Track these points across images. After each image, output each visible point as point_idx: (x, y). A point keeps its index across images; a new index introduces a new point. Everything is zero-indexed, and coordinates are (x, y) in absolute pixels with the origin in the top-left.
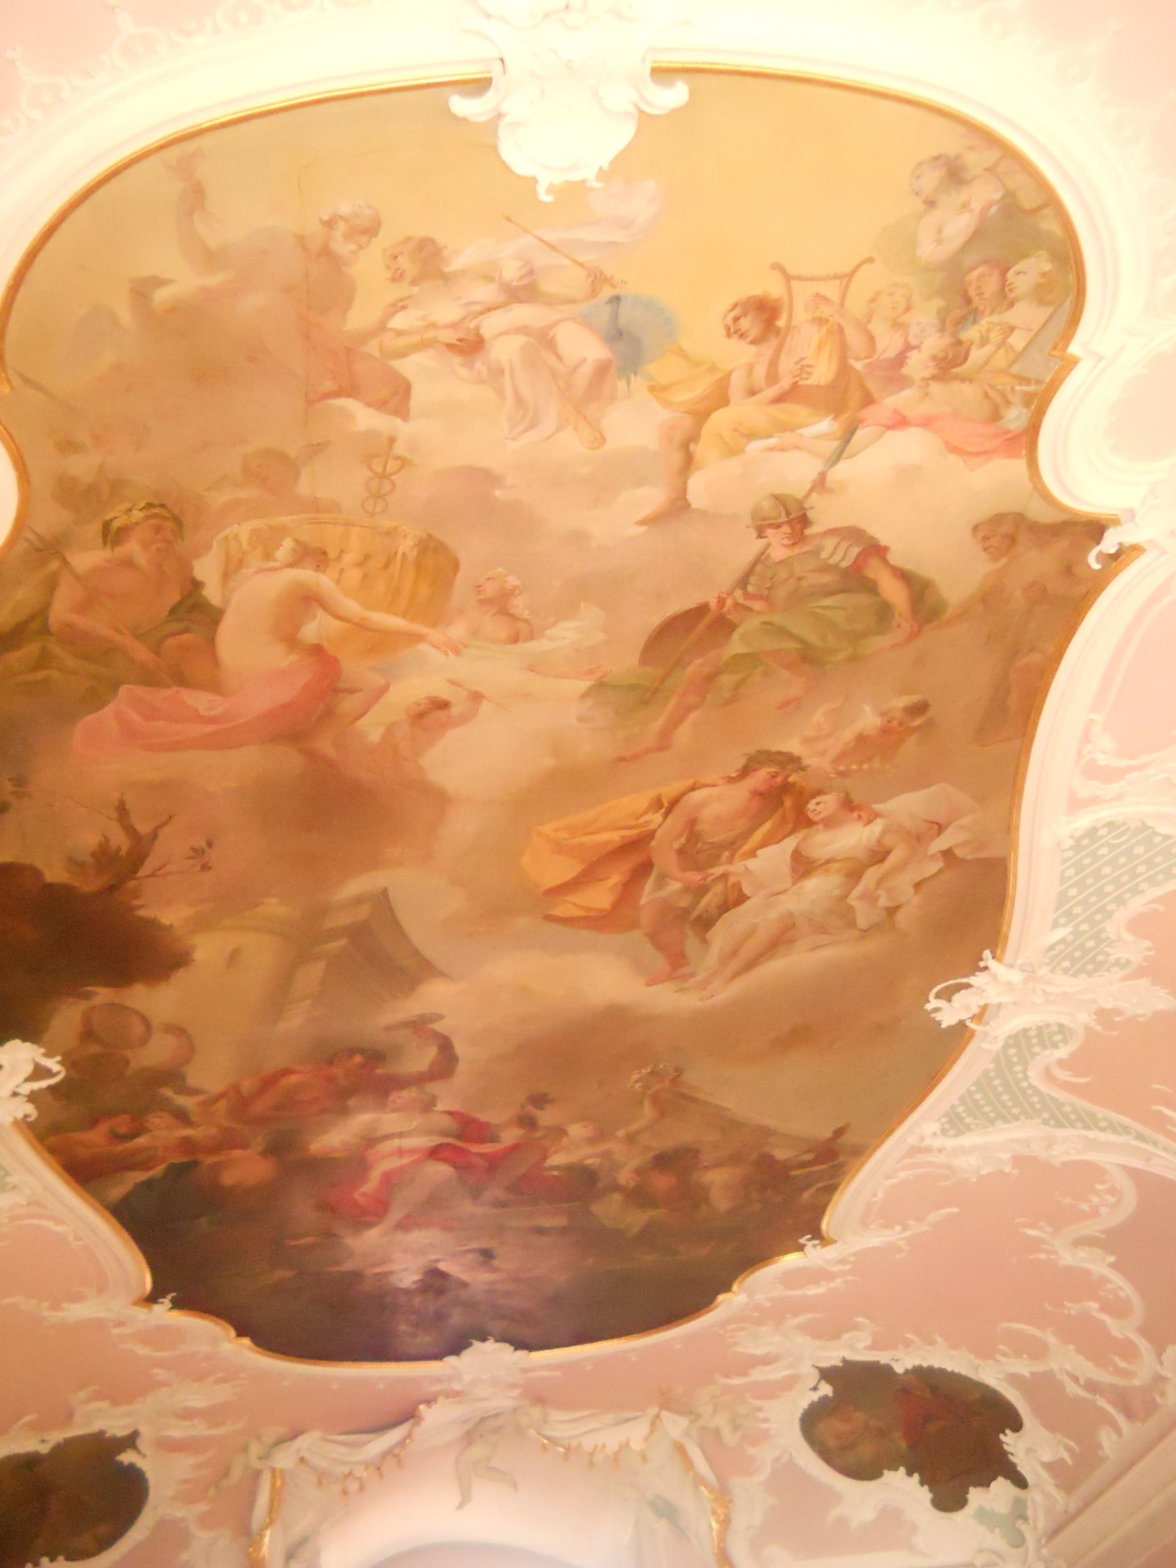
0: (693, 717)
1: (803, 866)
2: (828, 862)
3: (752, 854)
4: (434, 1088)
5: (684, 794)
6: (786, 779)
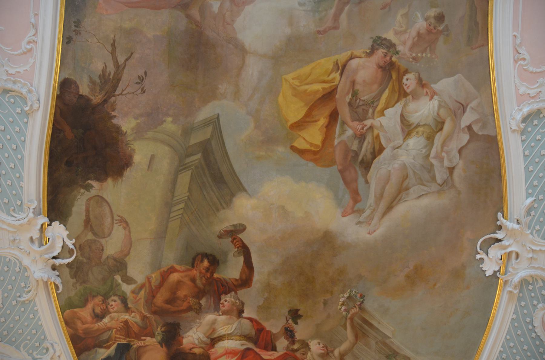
0: (347, 8)
1: (408, 128)
2: (418, 126)
3: (382, 114)
4: (242, 293)
6: (391, 59)
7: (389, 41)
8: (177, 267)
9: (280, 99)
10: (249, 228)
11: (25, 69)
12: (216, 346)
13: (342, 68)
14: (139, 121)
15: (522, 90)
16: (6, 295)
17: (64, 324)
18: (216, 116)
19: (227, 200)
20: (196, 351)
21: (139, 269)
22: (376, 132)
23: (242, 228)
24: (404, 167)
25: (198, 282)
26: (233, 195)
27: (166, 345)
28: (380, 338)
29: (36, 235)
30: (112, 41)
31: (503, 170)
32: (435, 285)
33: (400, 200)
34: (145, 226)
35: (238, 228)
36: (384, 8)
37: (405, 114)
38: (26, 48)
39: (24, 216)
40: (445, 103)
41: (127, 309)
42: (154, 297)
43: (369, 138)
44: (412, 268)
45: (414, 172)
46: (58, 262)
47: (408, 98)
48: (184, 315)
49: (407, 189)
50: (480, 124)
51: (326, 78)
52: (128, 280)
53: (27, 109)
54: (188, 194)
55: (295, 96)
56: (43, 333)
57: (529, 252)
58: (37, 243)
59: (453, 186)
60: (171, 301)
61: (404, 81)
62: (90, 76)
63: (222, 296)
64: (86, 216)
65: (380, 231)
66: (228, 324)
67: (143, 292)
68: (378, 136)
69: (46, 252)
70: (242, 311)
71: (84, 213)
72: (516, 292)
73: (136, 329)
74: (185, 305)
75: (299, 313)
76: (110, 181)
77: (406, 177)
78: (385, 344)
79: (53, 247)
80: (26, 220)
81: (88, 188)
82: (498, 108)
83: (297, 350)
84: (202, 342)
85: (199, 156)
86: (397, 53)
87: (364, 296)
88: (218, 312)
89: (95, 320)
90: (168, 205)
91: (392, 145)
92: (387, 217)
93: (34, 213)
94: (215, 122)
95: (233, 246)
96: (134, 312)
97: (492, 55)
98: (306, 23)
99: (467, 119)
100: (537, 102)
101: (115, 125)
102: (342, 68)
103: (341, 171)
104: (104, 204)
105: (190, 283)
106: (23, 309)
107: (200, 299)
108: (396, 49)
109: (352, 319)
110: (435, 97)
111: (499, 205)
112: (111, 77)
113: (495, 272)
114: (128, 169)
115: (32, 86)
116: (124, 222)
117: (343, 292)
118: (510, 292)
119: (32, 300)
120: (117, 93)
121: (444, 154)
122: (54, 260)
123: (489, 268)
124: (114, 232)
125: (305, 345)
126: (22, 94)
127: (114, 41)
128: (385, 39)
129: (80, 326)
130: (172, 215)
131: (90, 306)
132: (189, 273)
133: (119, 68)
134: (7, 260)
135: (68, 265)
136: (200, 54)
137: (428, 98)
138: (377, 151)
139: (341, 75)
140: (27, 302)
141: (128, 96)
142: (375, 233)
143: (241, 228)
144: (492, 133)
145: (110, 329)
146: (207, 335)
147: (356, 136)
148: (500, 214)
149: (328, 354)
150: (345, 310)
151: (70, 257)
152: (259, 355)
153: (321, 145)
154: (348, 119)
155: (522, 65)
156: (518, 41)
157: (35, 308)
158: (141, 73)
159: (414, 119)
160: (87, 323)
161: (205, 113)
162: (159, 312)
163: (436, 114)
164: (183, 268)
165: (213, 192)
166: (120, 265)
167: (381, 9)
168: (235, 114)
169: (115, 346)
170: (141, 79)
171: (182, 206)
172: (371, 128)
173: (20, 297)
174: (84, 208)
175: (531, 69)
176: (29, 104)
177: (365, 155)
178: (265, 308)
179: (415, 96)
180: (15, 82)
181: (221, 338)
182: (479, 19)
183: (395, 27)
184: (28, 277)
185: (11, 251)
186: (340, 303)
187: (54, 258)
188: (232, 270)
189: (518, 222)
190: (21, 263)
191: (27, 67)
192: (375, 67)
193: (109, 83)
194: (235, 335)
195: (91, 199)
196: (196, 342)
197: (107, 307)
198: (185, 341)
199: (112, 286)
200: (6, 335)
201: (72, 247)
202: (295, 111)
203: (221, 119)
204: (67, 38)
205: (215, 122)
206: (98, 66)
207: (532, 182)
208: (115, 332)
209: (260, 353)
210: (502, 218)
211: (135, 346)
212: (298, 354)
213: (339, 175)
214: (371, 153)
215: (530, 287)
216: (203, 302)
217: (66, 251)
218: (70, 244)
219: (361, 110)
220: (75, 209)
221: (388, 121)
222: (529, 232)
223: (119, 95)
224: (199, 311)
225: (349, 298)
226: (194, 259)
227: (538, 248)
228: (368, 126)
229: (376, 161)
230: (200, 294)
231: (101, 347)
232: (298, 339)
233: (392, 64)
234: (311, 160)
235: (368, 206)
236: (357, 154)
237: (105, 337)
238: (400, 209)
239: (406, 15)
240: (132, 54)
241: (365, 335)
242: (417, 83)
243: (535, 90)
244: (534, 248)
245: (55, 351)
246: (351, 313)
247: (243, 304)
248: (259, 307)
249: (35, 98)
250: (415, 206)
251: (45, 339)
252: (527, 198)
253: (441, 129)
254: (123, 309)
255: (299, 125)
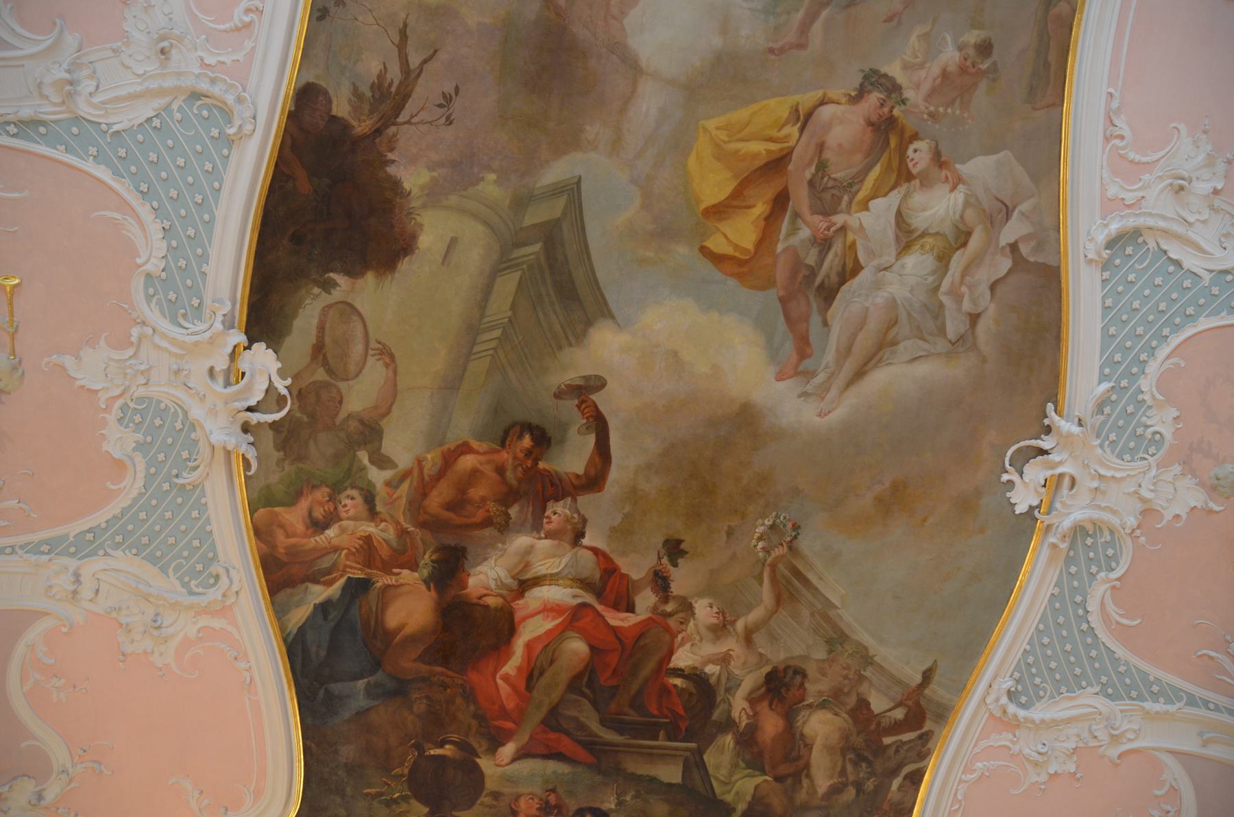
0: (825, 13)
1: (907, 236)
2: (924, 234)
4: (584, 501)
5: (816, 107)
7: (892, 80)
8: (475, 444)
9: (692, 161)
10: (611, 385)
11: (235, 58)
12: (527, 594)
13: (804, 118)
14: (435, 174)
15: (1112, 191)
16: (153, 470)
17: (252, 533)
18: (576, 180)
19: (578, 330)
20: (491, 601)
21: (404, 443)
22: (851, 237)
23: (597, 384)
24: (892, 303)
25: (509, 474)
26: (589, 323)
27: (436, 587)
28: (820, 607)
29: (221, 364)
30: (401, 25)
31: (1064, 329)
32: (925, 520)
33: (880, 361)
34: (425, 364)
35: (592, 383)
36: (889, 19)
37: (904, 211)
38: (241, 20)
39: (203, 327)
40: (977, 199)
41: (373, 514)
42: (425, 495)
43: (837, 247)
44: (887, 485)
45: (909, 315)
46: (255, 418)
47: (913, 183)
48: (476, 533)
49: (894, 343)
50: (1033, 243)
51: (774, 133)
52: (382, 461)
53: (231, 131)
54: (510, 313)
55: (718, 158)
56: (213, 547)
57: (1093, 479)
58: (221, 380)
59: (975, 347)
60: (454, 506)
61: (910, 152)
62: (354, 84)
63: (550, 504)
64: (318, 337)
65: (839, 414)
66: (554, 556)
67: (405, 486)
68: (854, 243)
69: (236, 397)
70: (581, 535)
71: (314, 332)
72: (1064, 546)
73: (384, 552)
74: (480, 515)
75: (683, 546)
76: (370, 277)
77: (894, 322)
78: (827, 618)
79: (249, 389)
80: (208, 335)
81: (328, 286)
82: (1067, 216)
83: (670, 615)
84: (503, 585)
85: (537, 247)
86: (903, 102)
87: (799, 527)
88: (538, 532)
89: (310, 531)
90: (473, 330)
91: (876, 262)
92: (853, 390)
93: (223, 323)
94: (572, 191)
95: (580, 414)
96: (385, 521)
97: (1067, 124)
98: (751, 33)
99: (1013, 231)
100: (1136, 215)
101: (391, 177)
102: (804, 118)
103: (782, 300)
104: (355, 318)
105: (493, 475)
106: (179, 500)
107: (508, 506)
108: (901, 94)
109: (773, 567)
110: (961, 187)
111: (1052, 391)
112: (393, 89)
113: (1031, 508)
114: (407, 259)
115: (244, 91)
116: (387, 355)
117: (764, 516)
118: (1054, 546)
119: (198, 486)
120: (401, 119)
121: (964, 289)
122: (249, 414)
123: (1022, 500)
124: (364, 371)
125: (687, 607)
126: (225, 103)
127: (405, 26)
128: (885, 76)
129: (282, 540)
130: (476, 349)
131: (304, 504)
132: (495, 456)
133: (410, 76)
134: (162, 406)
135: (274, 426)
136: (557, 65)
137: (947, 187)
138: (850, 270)
139: (802, 130)
140: (188, 488)
141: (421, 127)
142: (831, 415)
143: (598, 383)
144: (1052, 262)
145: (336, 549)
146: (516, 571)
147: (815, 241)
148: (1050, 406)
149: (724, 626)
150: (763, 548)
151: (278, 411)
152: (603, 617)
153: (752, 250)
154: (805, 210)
155: (1118, 148)
156: (1115, 104)
157: (203, 501)
158: (449, 88)
159: (919, 221)
160: (295, 535)
161: (556, 172)
162: (431, 525)
163: (957, 216)
164: (484, 446)
165: (555, 313)
166: (369, 432)
167: (885, 21)
168: (608, 179)
169: (342, 581)
170: (448, 99)
171: (497, 333)
172: (843, 229)
173: (177, 476)
174: (315, 322)
175: (1132, 156)
176: (237, 122)
177: (828, 276)
178: (623, 532)
179: (926, 182)
180: (213, 81)
181: (537, 581)
182: (1053, 57)
183: (905, 57)
184: (196, 442)
185: (172, 391)
186: (757, 535)
187: (250, 409)
188: (572, 459)
189: (1080, 423)
190: (185, 413)
191: (240, 56)
192: (862, 122)
193: (389, 101)
194: (565, 578)
195: (329, 306)
196: (493, 585)
197: (336, 508)
198: (472, 582)
199: (349, 469)
200: (196, 518)
201: (284, 392)
202: (714, 186)
203: (583, 186)
204: (319, 10)
205: (572, 191)
206: (371, 67)
207: (1112, 355)
208: (347, 556)
209: (605, 614)
210: (1053, 413)
211: (379, 585)
212: (672, 622)
213: (778, 305)
214: (838, 274)
215: (1089, 541)
216: (513, 511)
217: (272, 399)
218: (281, 386)
219: (830, 195)
220: (298, 323)
221: (873, 220)
222: (1098, 442)
223: (404, 123)
224: (504, 527)
225: (772, 527)
226: (506, 433)
227: (1109, 474)
228: (838, 226)
229: (845, 288)
230: (509, 496)
231: (316, 581)
232: (675, 593)
233: (891, 121)
234: (732, 275)
235: (823, 365)
236: (813, 272)
237: (326, 563)
238: (879, 378)
239: (926, 37)
240: (436, 51)
241: (793, 598)
242: (932, 159)
243: (1135, 194)
244: (1102, 472)
245: (231, 581)
246: (773, 555)
247: (584, 521)
248: (613, 530)
249: (248, 114)
250: (904, 376)
251: (214, 558)
252: (1100, 383)
253: (964, 244)
254: (365, 514)
255: (719, 211)
